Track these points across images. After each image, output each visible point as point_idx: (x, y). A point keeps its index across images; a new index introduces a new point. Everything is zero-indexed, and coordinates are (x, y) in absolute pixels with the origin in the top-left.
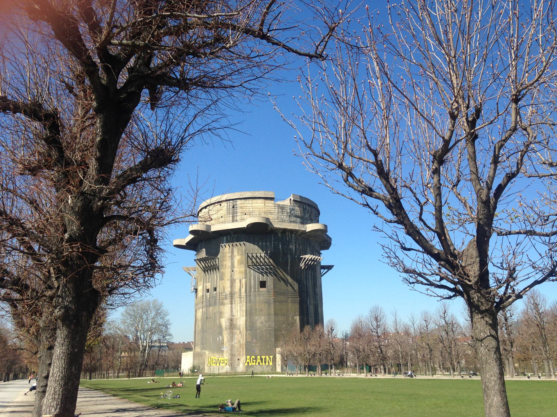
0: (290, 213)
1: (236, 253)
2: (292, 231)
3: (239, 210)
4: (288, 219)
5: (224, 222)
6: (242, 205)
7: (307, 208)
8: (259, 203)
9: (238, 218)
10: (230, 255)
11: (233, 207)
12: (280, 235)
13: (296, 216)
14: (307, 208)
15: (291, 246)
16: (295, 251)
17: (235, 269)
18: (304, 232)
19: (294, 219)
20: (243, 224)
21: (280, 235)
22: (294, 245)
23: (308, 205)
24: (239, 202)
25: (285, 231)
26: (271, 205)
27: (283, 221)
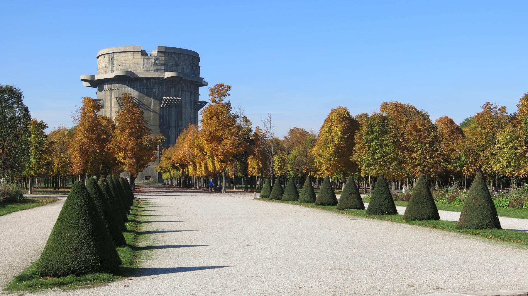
0: (155, 62)
1: (113, 97)
2: (155, 79)
3: (115, 62)
4: (152, 67)
5: (106, 72)
6: (118, 58)
7: (173, 56)
8: (129, 56)
9: (115, 68)
10: (110, 98)
11: (112, 59)
12: (145, 81)
13: (161, 65)
14: (173, 56)
15: (154, 90)
16: (158, 94)
17: (113, 109)
18: (163, 79)
19: (157, 67)
20: (111, 76)
21: (145, 81)
22: (157, 88)
23: (174, 53)
24: (115, 55)
25: (147, 79)
26: (138, 57)
27: (148, 70)
